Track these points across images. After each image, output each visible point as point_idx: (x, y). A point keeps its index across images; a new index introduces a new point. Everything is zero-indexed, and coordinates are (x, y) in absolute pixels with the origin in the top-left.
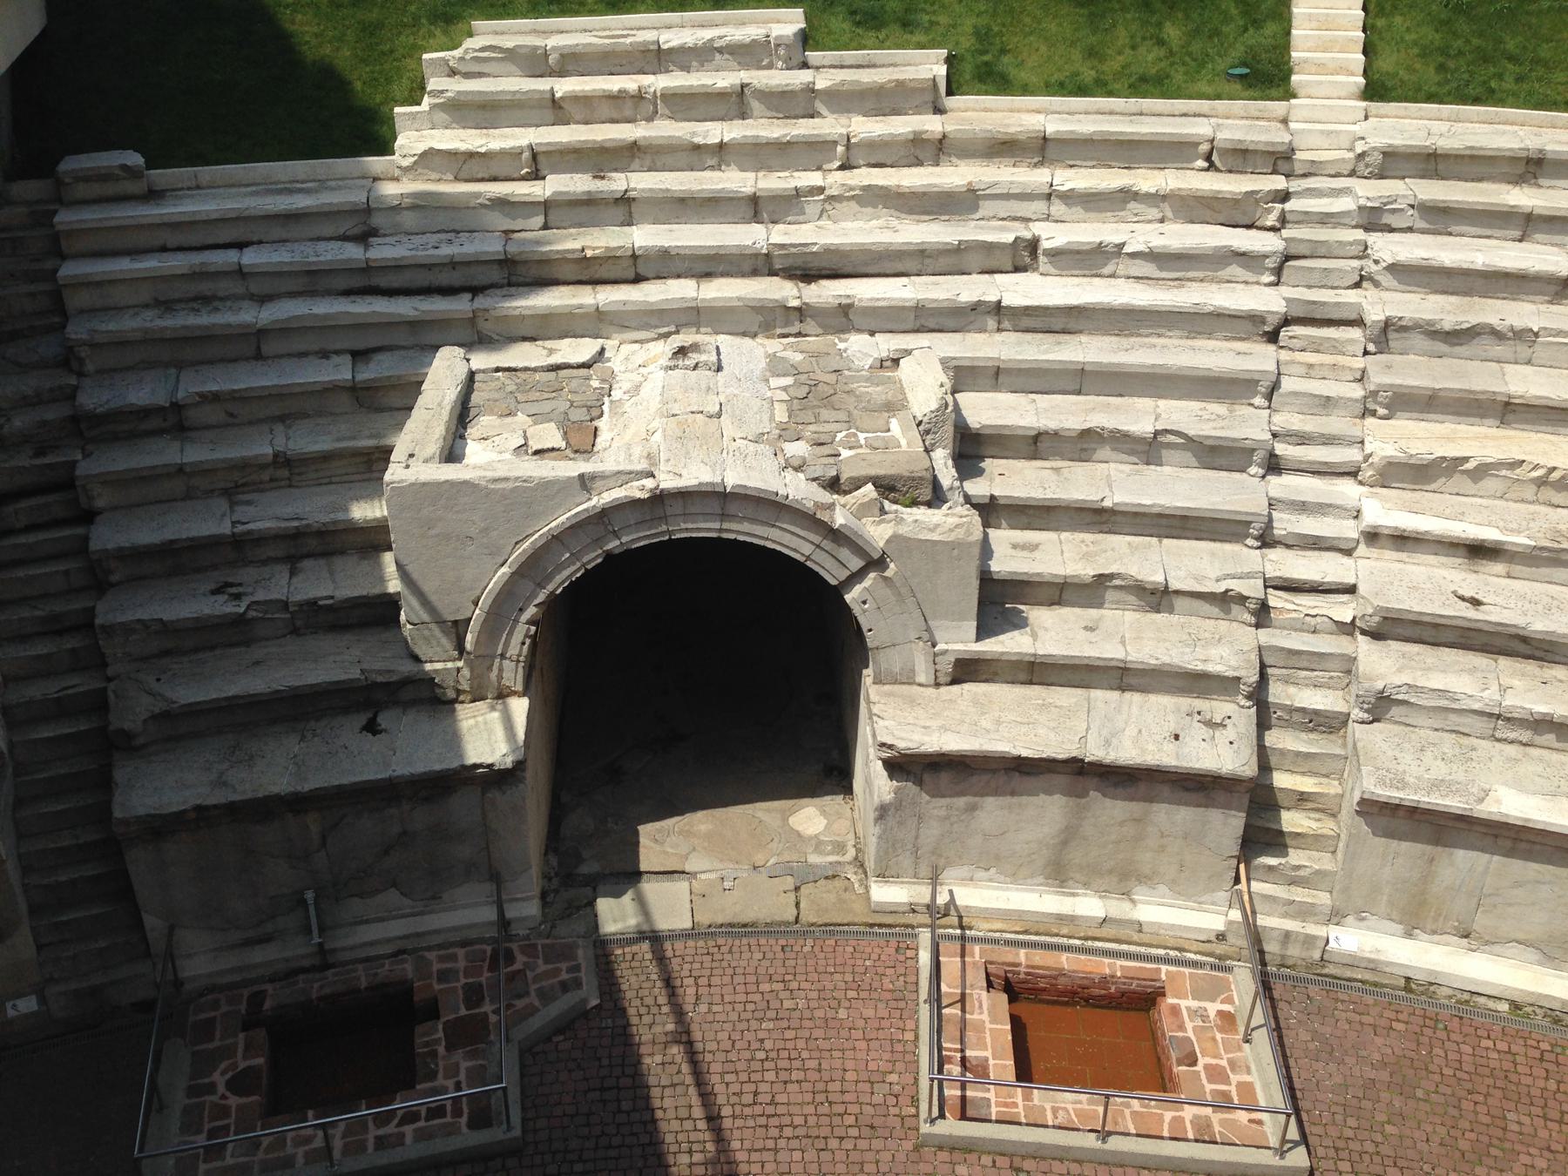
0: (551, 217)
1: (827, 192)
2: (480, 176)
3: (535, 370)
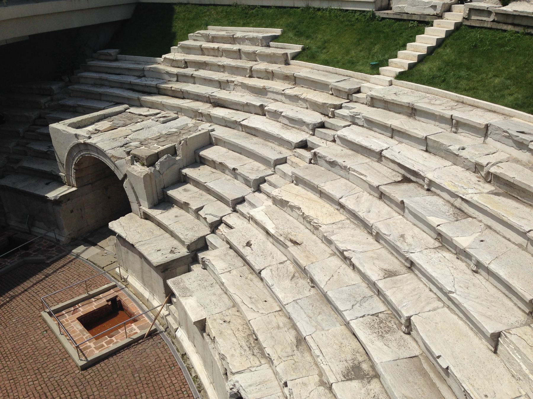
0: (179, 79)
1: (235, 83)
2: (176, 66)
3: (136, 114)
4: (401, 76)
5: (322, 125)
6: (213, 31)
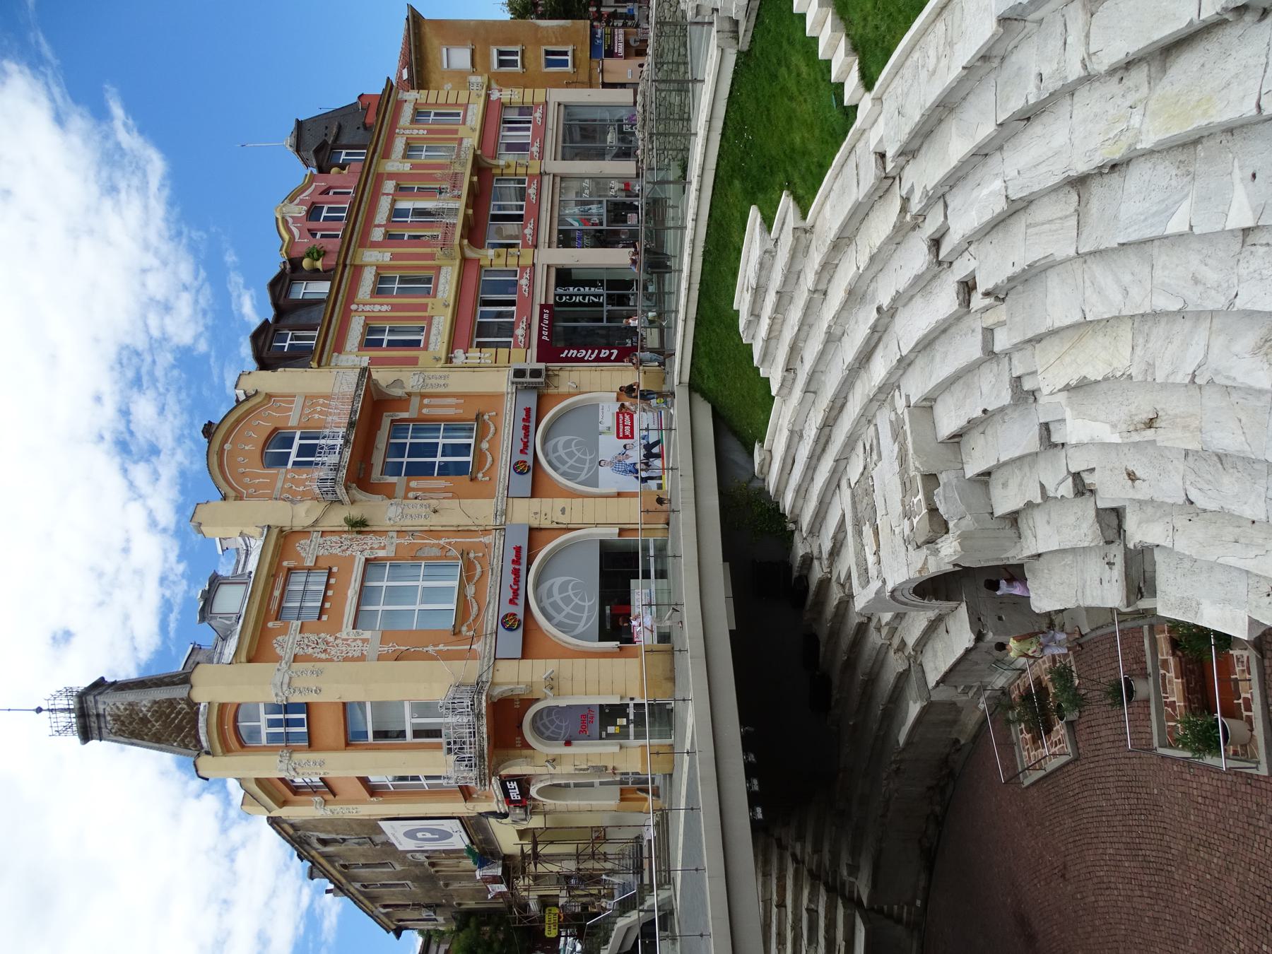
4: (868, 81)
5: (936, 243)
6: (742, 302)
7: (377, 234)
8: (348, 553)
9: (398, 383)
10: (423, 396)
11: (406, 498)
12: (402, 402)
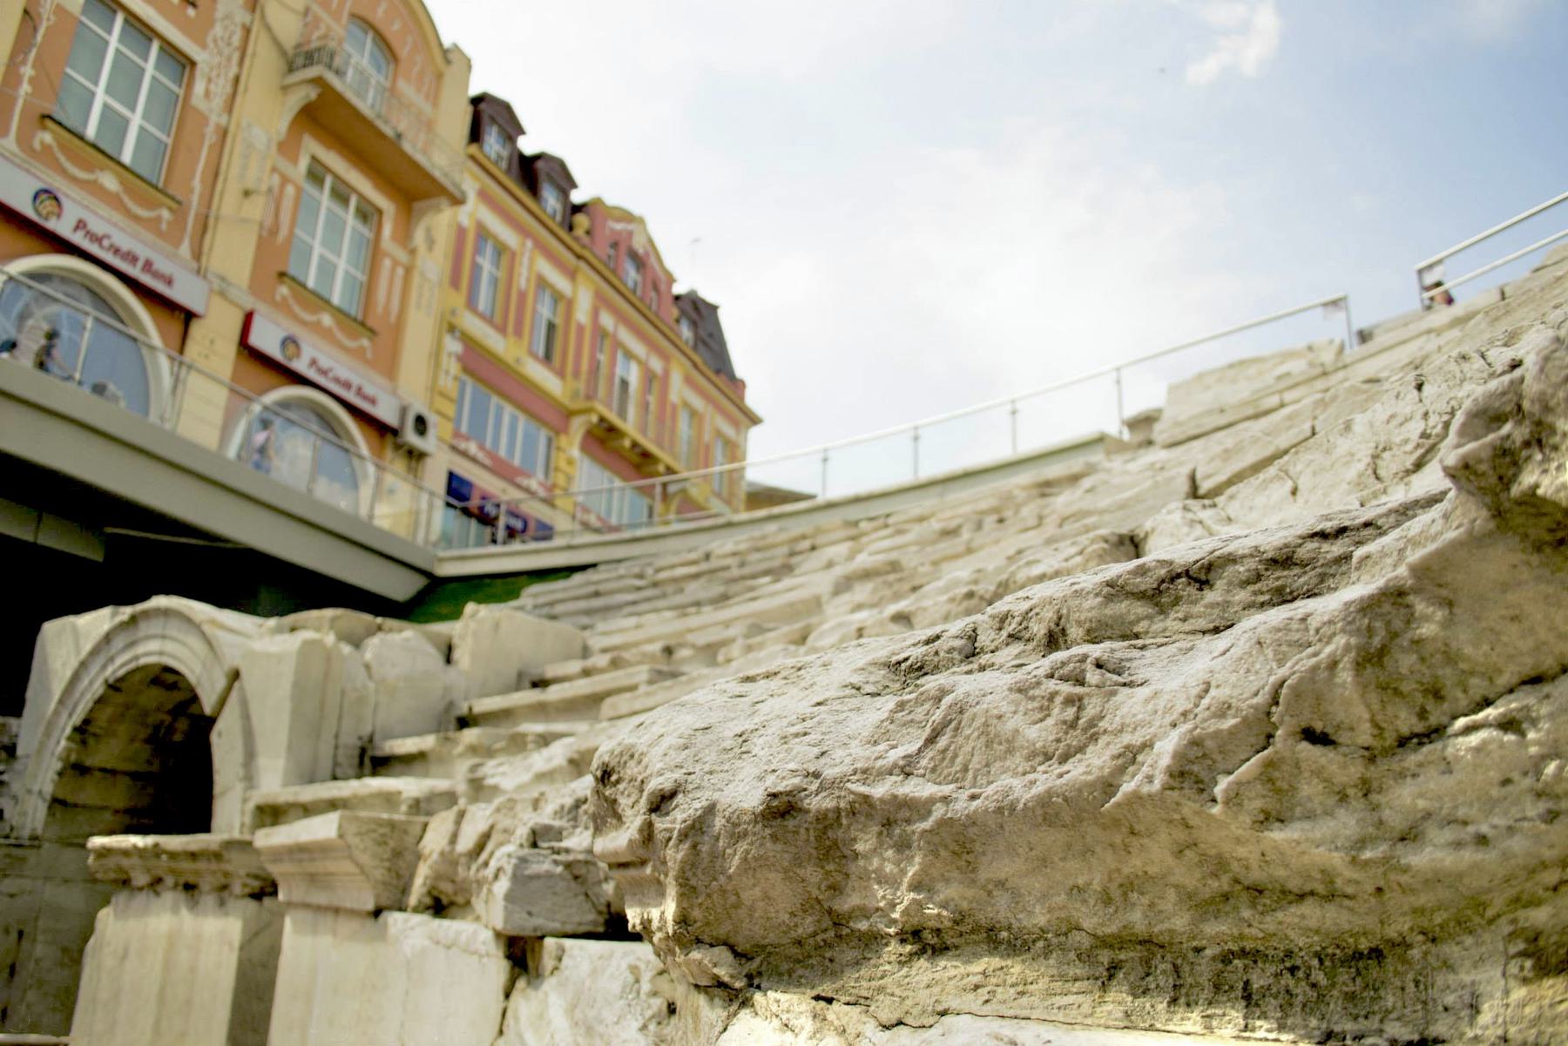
7: (607, 320)
8: (211, 45)
9: (431, 243)
10: (409, 270)
11: (274, 170)
12: (404, 235)
